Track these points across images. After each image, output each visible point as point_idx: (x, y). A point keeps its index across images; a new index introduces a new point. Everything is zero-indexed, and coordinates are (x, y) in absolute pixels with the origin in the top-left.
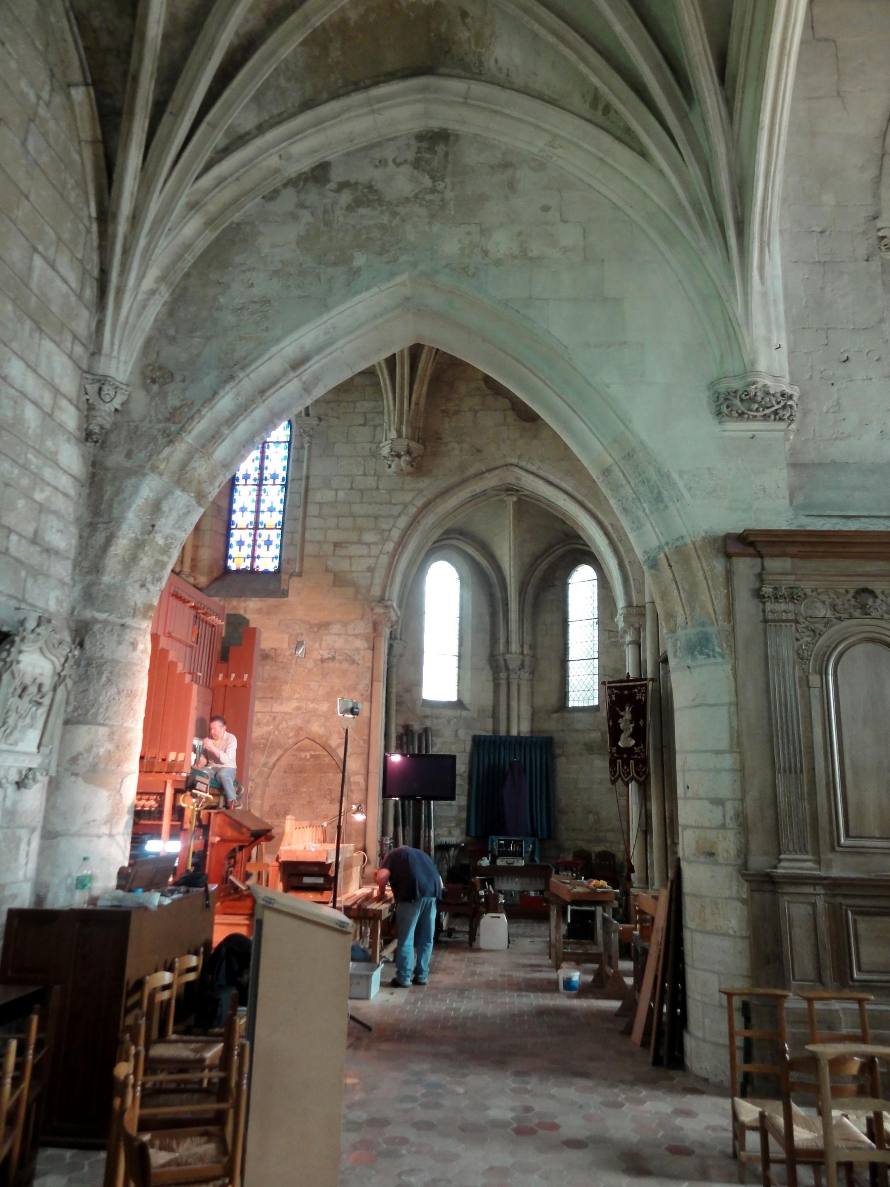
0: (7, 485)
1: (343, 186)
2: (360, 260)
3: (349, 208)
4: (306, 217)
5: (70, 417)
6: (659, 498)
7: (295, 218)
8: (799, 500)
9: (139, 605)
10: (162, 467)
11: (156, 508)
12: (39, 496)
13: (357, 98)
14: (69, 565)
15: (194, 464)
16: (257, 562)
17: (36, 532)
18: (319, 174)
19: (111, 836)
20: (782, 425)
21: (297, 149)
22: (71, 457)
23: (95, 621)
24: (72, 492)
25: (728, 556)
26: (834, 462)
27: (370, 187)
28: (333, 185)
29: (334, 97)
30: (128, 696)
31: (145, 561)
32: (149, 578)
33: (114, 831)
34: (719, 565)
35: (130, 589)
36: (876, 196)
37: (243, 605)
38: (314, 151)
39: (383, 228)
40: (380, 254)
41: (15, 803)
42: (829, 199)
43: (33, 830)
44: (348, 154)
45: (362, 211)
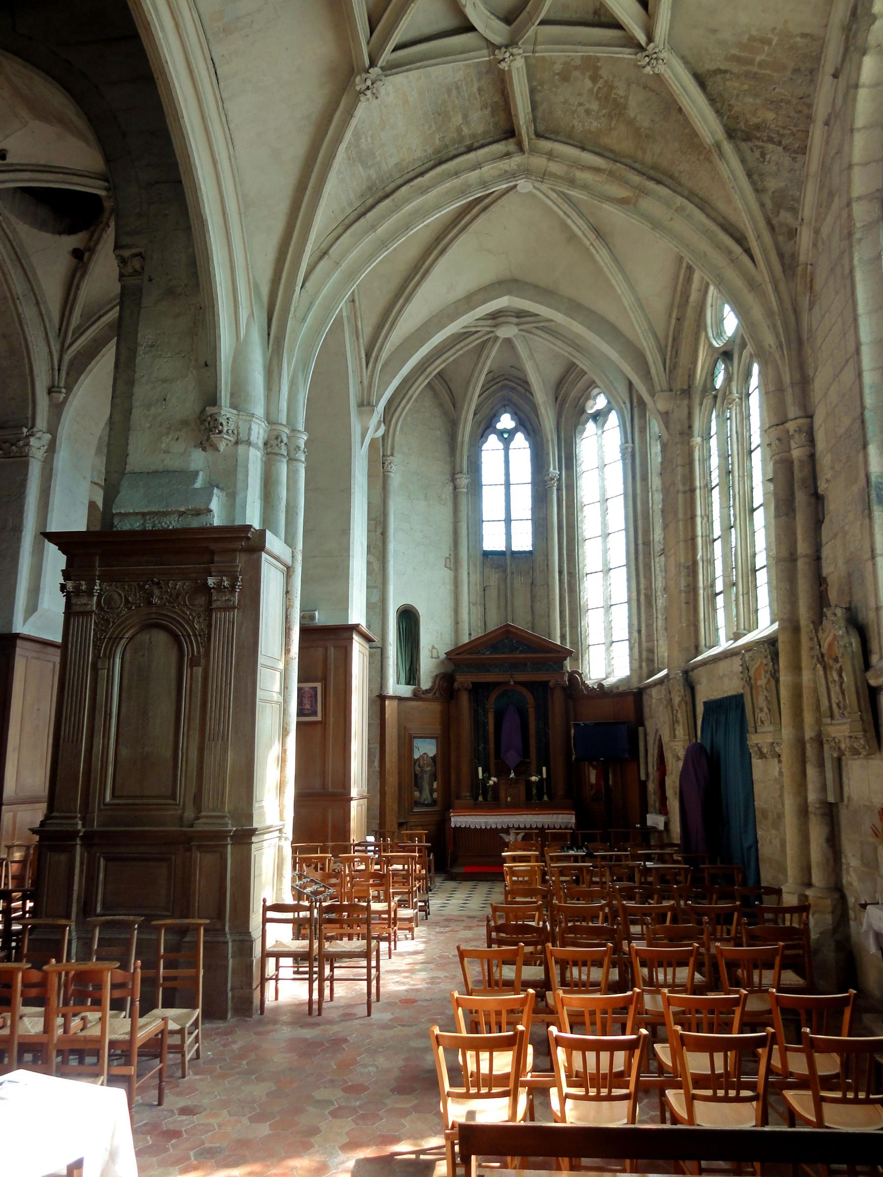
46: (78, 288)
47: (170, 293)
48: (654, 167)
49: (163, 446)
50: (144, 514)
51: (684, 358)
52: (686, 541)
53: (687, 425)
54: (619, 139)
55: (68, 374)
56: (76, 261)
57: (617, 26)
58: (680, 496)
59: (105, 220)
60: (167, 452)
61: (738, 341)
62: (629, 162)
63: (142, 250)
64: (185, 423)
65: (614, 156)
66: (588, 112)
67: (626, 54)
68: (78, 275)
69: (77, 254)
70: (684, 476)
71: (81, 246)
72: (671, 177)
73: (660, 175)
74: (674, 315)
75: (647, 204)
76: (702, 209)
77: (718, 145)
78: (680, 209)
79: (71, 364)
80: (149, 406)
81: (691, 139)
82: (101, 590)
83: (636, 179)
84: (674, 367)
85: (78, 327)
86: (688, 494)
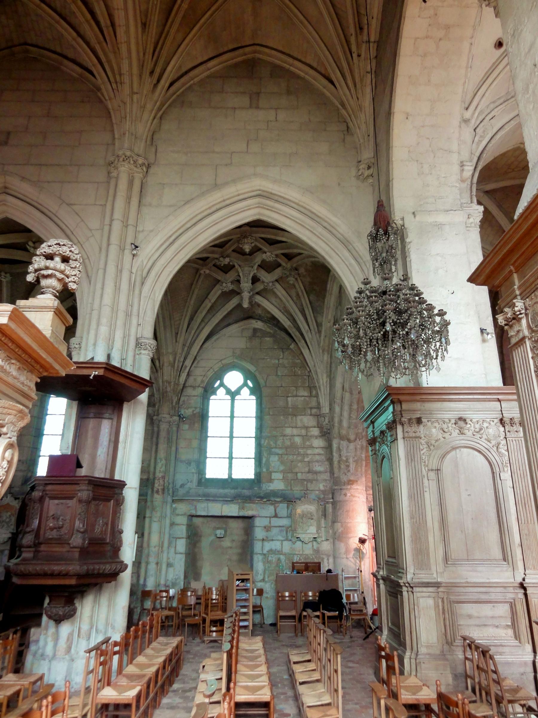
0: (292, 462)
5: (316, 432)
9: (346, 480)
10: (335, 436)
11: (339, 450)
12: (306, 460)
14: (328, 474)
15: (341, 431)
17: (309, 470)
19: (347, 558)
21: (330, 317)
22: (319, 443)
23: (335, 489)
24: (323, 452)
30: (346, 512)
31: (342, 466)
32: (346, 471)
33: (348, 557)
35: (341, 477)
41: (318, 548)
43: (328, 556)
82: (526, 309)
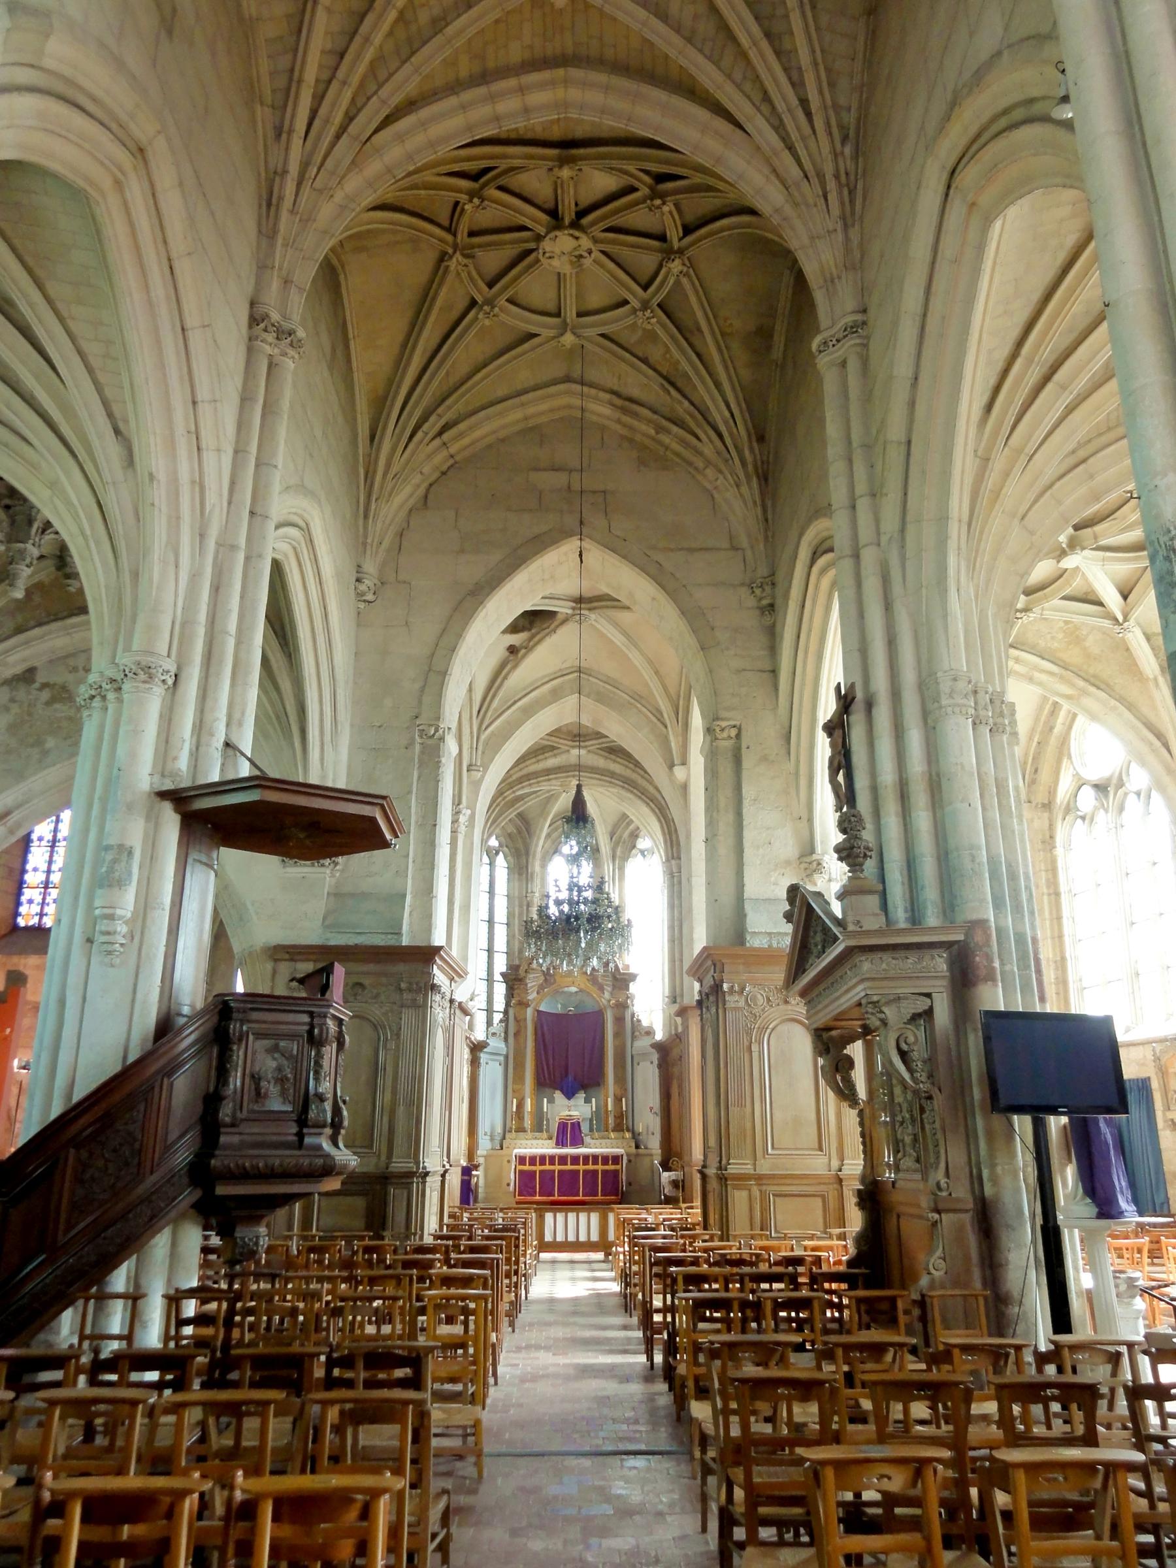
1: (45, 686)
2: (50, 743)
3: (48, 703)
4: (15, 709)
6: (241, 919)
7: (7, 709)
8: (327, 923)
13: (54, 626)
16: (45, 919)
18: (28, 676)
20: (322, 870)
25: (276, 960)
26: (363, 894)
27: (64, 688)
28: (37, 685)
29: (40, 625)
34: (269, 966)
36: (420, 702)
37: (23, 961)
38: (24, 660)
39: (70, 719)
40: (65, 739)
42: (388, 702)
44: (51, 661)
45: (57, 706)
46: (505, 678)
47: (764, 759)
48: (1094, 676)
49: (773, 879)
50: (770, 934)
51: (1044, 776)
52: (1053, 938)
53: (1048, 837)
54: (1073, 656)
55: (483, 753)
56: (507, 654)
57: (1101, 604)
58: (1045, 897)
59: (553, 626)
60: (775, 884)
61: (1114, 781)
62: (1075, 670)
63: (738, 723)
64: (788, 863)
65: (1065, 667)
66: (1053, 638)
67: (1107, 623)
68: (509, 666)
69: (512, 650)
70: (1048, 880)
71: (517, 644)
72: (1108, 685)
73: (1097, 682)
74: (1036, 740)
75: (1087, 701)
76: (1130, 710)
77: (1156, 679)
78: (1114, 709)
79: (486, 743)
80: (758, 847)
81: (1132, 667)
83: (1081, 683)
84: (1033, 782)
85: (496, 710)
86: (1053, 897)
